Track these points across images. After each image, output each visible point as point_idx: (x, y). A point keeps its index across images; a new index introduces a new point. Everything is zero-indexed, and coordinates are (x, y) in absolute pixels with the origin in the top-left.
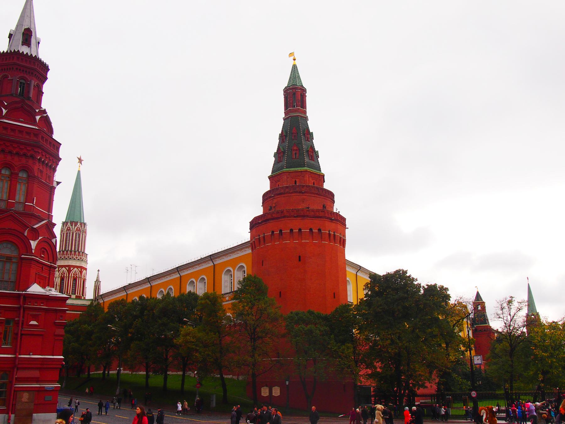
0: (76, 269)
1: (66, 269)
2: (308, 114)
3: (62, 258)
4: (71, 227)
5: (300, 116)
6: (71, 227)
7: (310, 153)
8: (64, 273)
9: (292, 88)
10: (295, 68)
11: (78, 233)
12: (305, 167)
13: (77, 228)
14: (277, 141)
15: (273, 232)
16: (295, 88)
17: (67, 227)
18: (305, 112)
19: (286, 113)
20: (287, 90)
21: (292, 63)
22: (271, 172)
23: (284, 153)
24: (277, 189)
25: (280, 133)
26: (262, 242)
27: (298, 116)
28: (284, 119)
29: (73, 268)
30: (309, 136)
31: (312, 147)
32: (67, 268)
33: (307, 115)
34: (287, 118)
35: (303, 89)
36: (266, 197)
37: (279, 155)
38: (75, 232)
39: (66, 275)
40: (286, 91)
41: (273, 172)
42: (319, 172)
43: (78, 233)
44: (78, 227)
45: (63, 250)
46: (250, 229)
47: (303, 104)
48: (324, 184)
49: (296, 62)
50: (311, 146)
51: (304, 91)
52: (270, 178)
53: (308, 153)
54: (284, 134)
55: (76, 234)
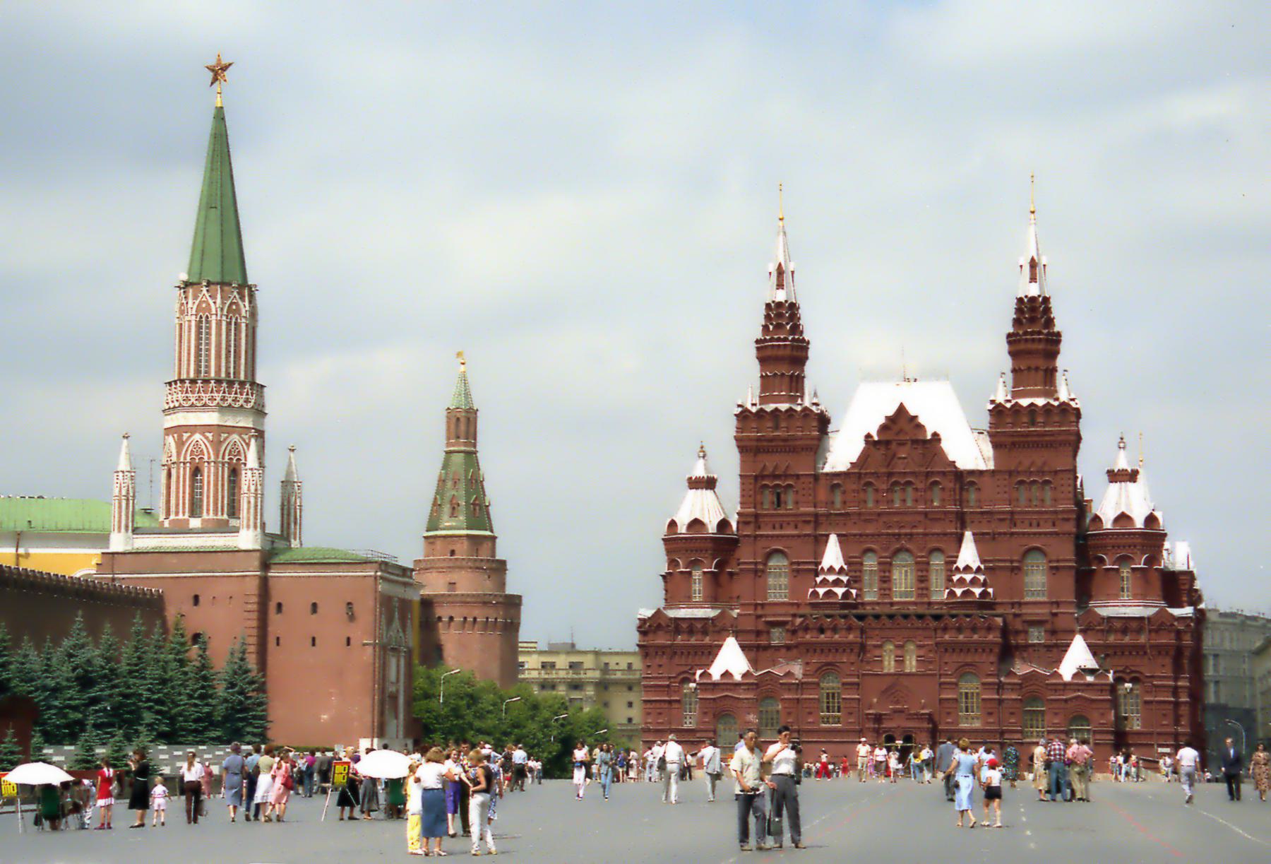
0: (197, 437)
1: (207, 438)
3: (190, 403)
4: (211, 302)
6: (211, 302)
8: (239, 452)
11: (234, 320)
13: (232, 304)
17: (197, 302)
29: (189, 434)
32: (210, 435)
38: (224, 318)
39: (209, 458)
43: (234, 320)
44: (235, 301)
45: (192, 375)
55: (229, 324)
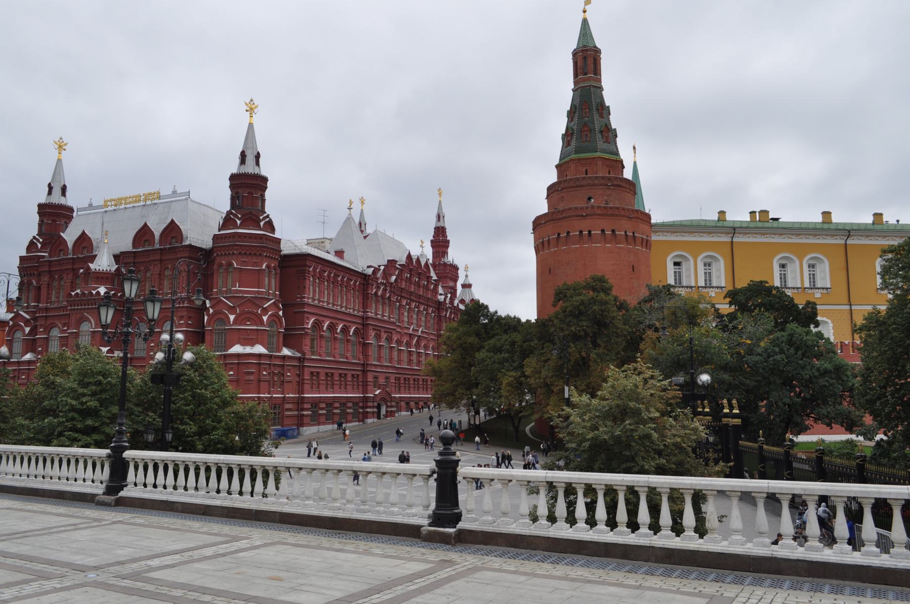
2: (604, 83)
5: (594, 86)
9: (583, 51)
10: (585, 22)
15: (559, 234)
16: (587, 50)
18: (600, 81)
19: (575, 83)
22: (558, 160)
23: (572, 134)
24: (565, 181)
26: (546, 244)
28: (574, 91)
34: (577, 89)
36: (552, 190)
37: (567, 137)
40: (575, 54)
41: (560, 160)
42: (616, 157)
46: (533, 230)
47: (597, 71)
48: (624, 170)
49: (587, 15)
50: (606, 125)
51: (597, 52)
52: (557, 167)
54: (573, 109)
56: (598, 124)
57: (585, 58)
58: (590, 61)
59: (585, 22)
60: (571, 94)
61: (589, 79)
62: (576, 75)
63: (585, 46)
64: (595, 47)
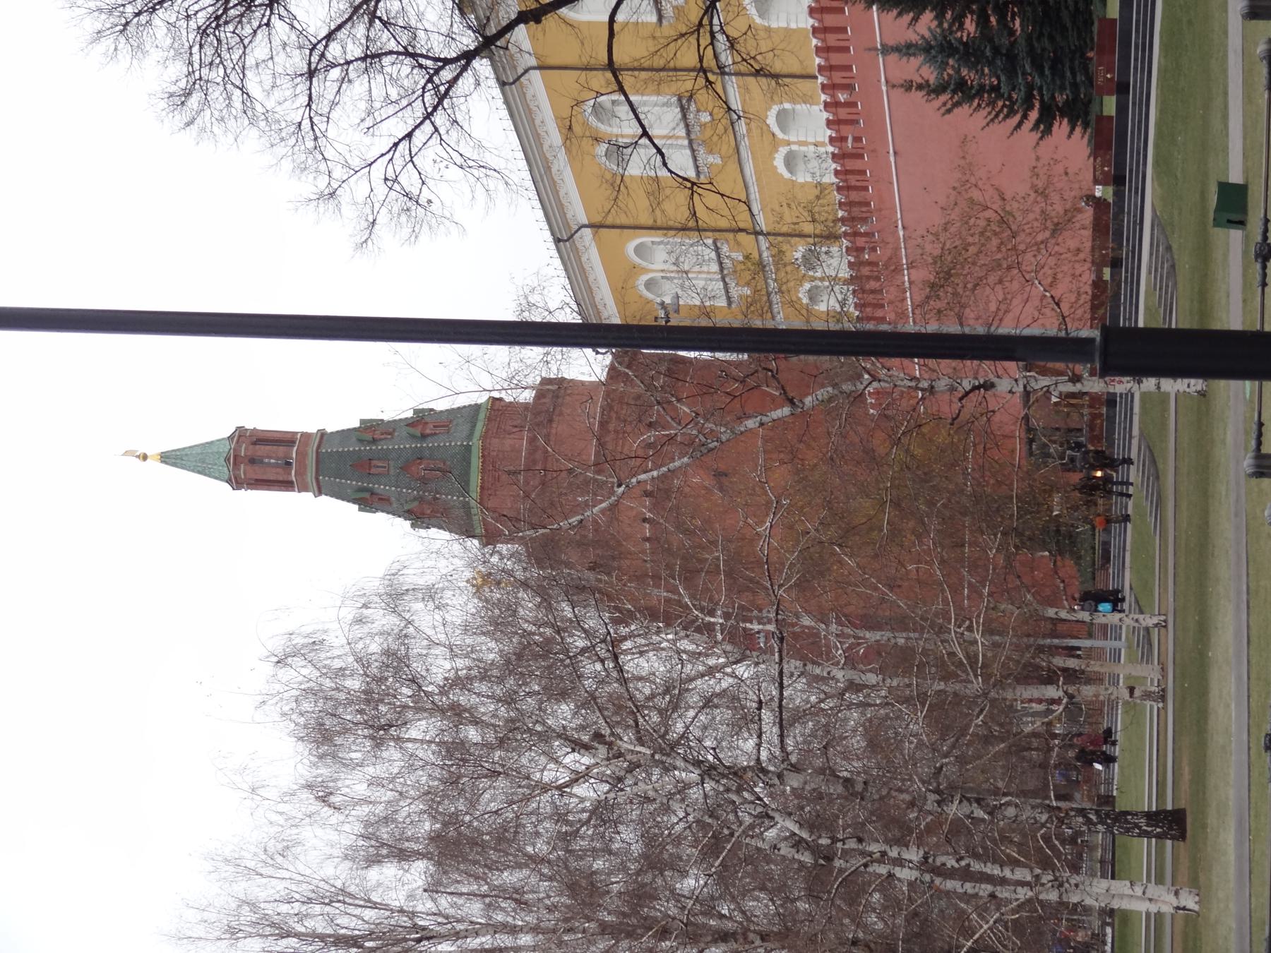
7: (428, 431)
9: (235, 463)
10: (171, 458)
12: (468, 448)
14: (381, 518)
18: (306, 436)
19: (304, 488)
20: (236, 478)
21: (154, 465)
25: (356, 507)
27: (317, 452)
28: (320, 492)
30: (372, 430)
31: (410, 423)
33: (315, 431)
35: (240, 436)
40: (237, 483)
47: (283, 440)
49: (154, 449)
51: (241, 435)
53: (428, 435)
54: (367, 495)
56: (403, 444)
57: (252, 461)
58: (262, 450)
59: (171, 458)
60: (328, 503)
61: (302, 455)
62: (286, 485)
63: (227, 459)
64: (231, 438)
